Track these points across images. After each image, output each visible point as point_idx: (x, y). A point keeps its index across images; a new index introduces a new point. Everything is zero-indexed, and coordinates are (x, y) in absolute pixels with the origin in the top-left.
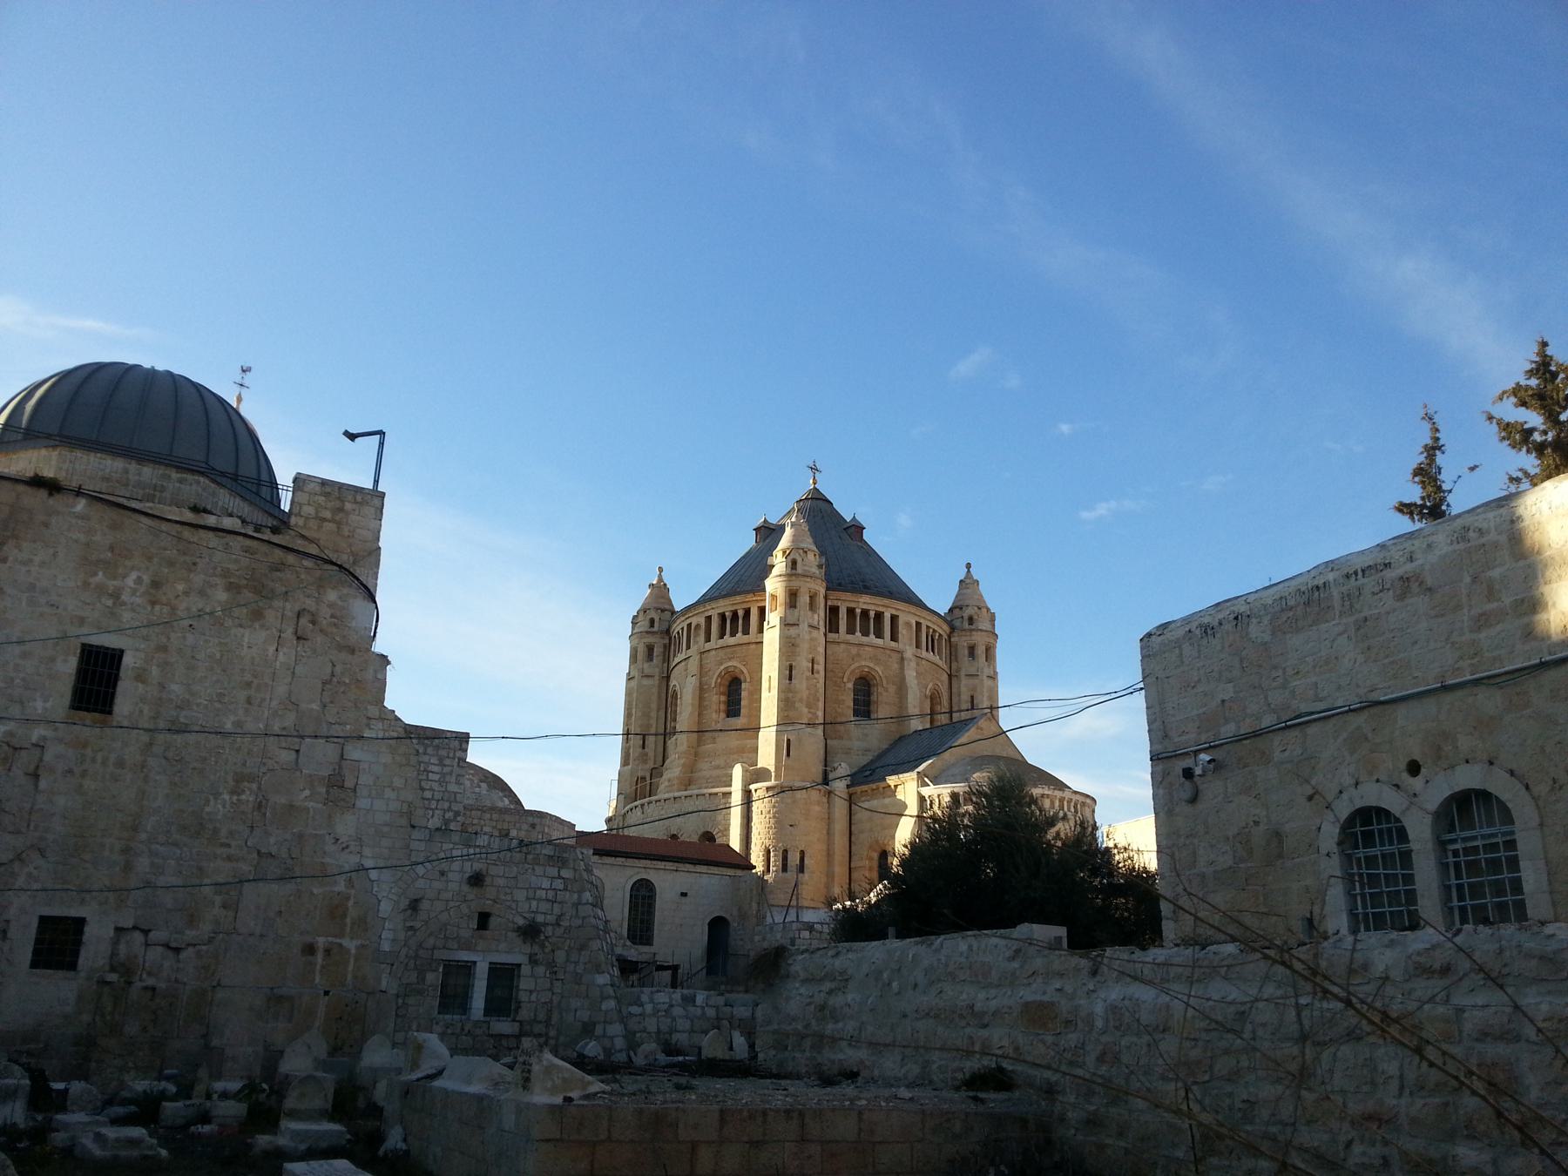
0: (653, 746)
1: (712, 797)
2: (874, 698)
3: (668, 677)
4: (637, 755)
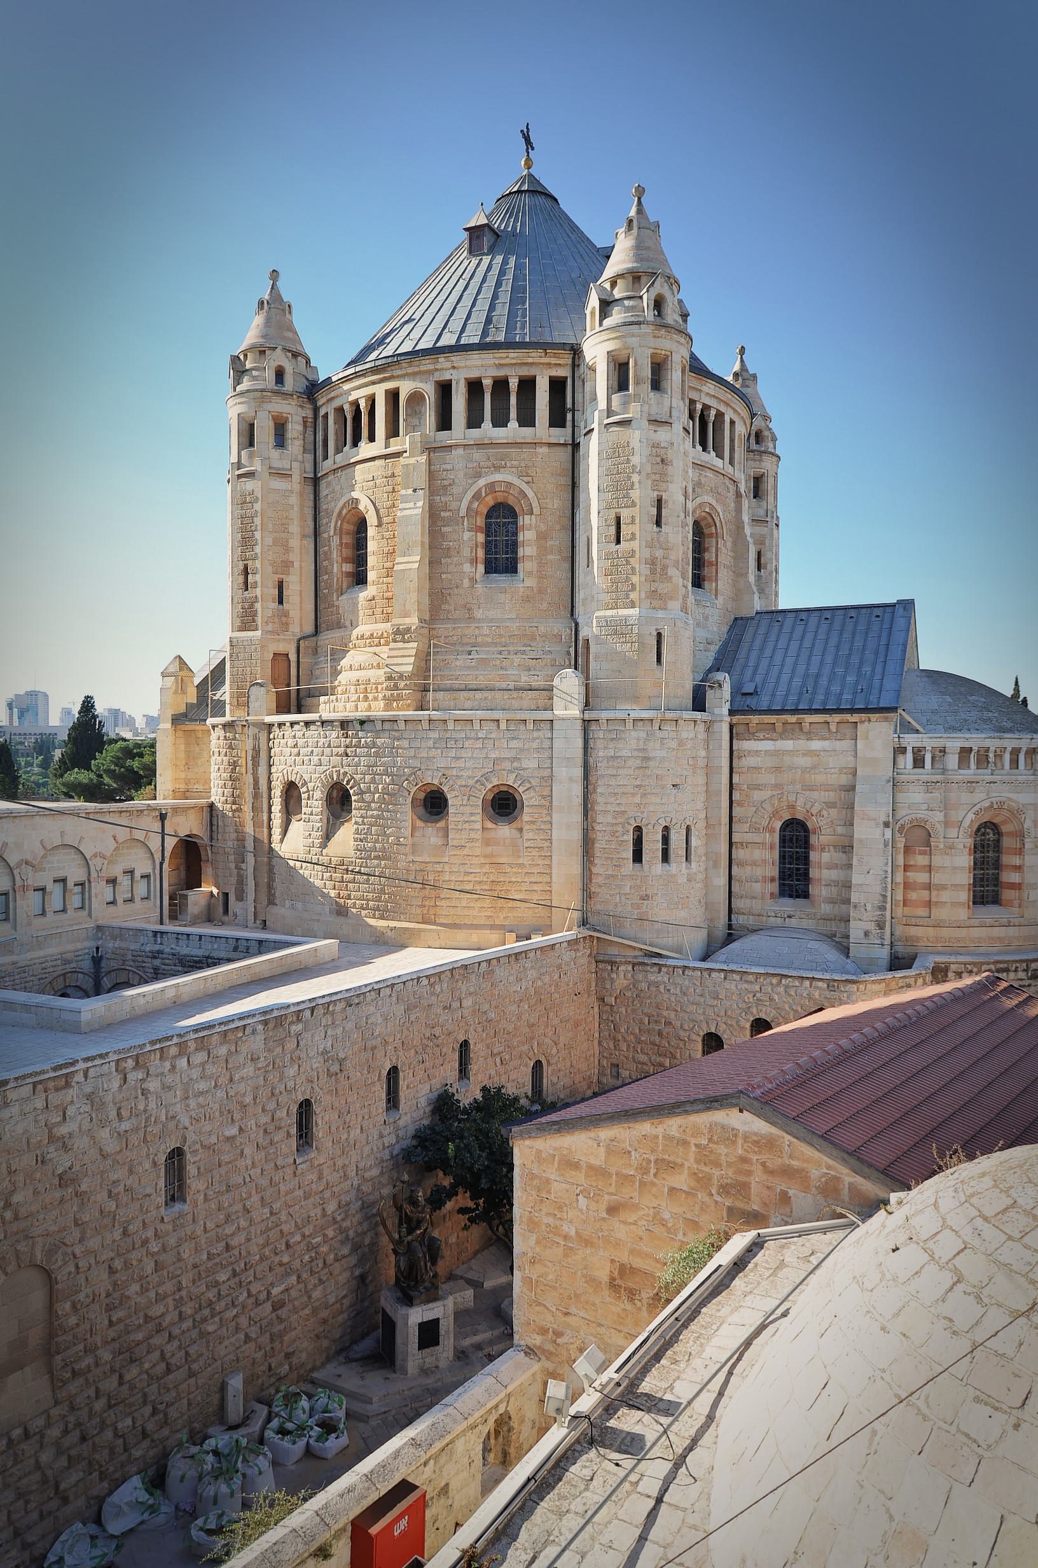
2: (709, 556)
3: (315, 481)
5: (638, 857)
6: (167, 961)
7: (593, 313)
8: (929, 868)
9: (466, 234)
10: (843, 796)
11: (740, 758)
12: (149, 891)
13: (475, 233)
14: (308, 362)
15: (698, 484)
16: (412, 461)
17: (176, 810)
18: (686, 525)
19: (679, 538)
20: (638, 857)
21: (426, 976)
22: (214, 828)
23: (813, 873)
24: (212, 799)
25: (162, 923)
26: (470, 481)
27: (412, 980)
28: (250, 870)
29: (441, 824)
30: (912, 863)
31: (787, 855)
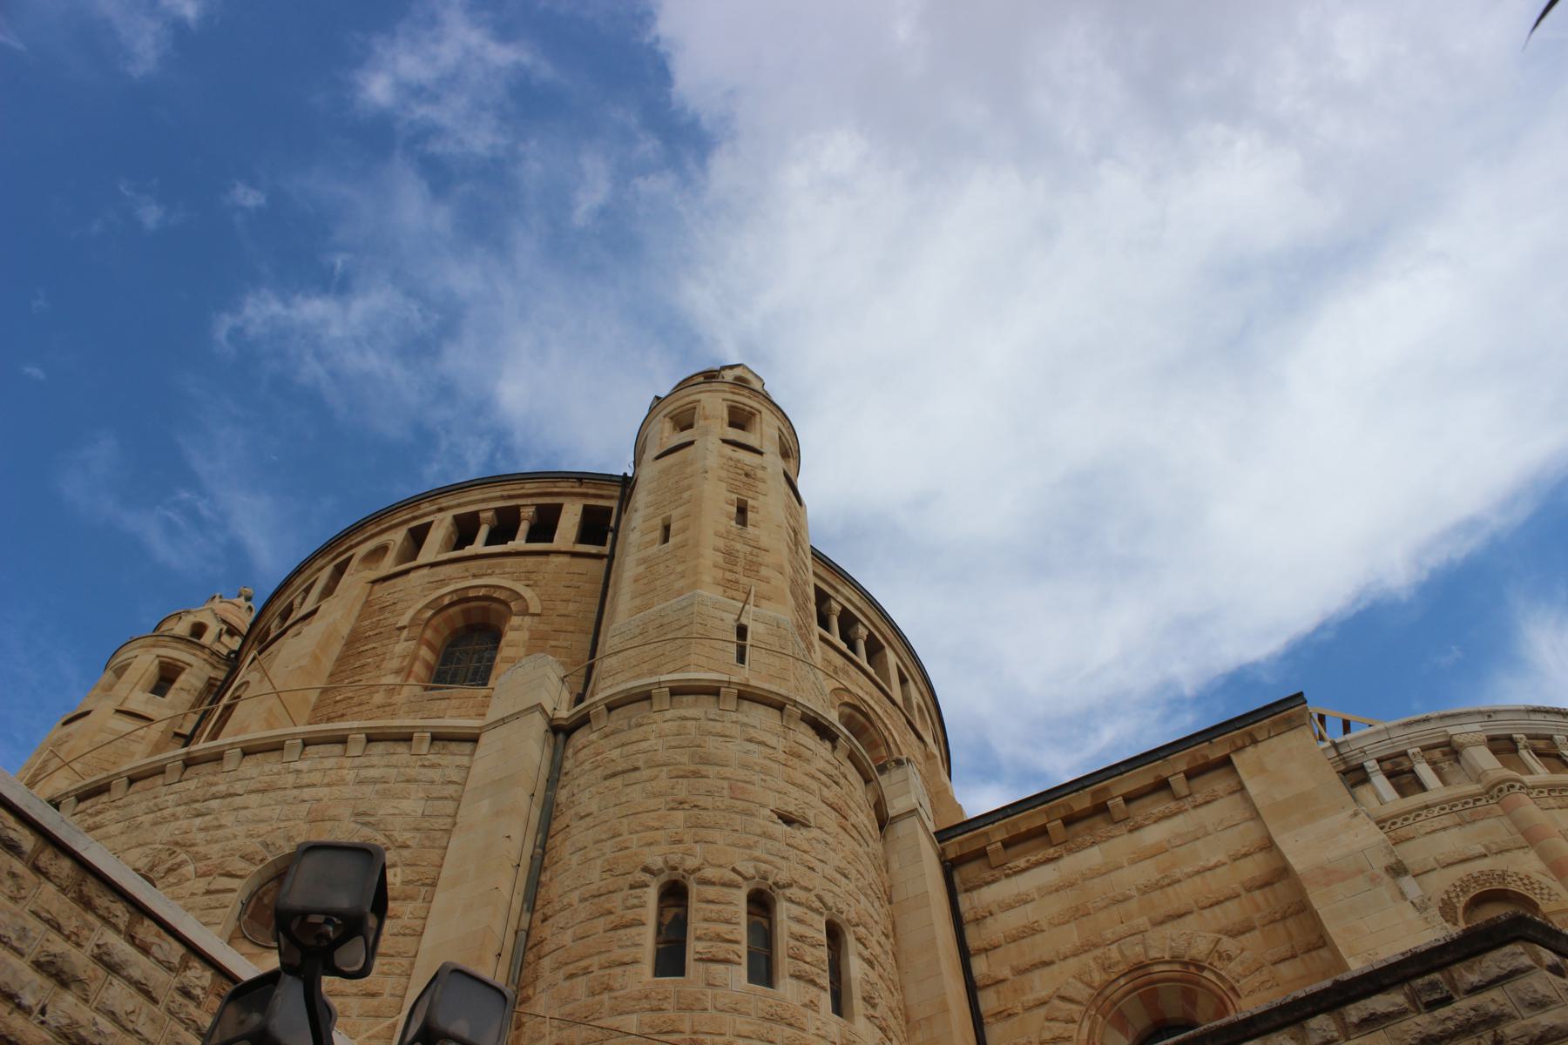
1: (379, 748)
5: (671, 959)
11: (978, 920)
20: (671, 959)
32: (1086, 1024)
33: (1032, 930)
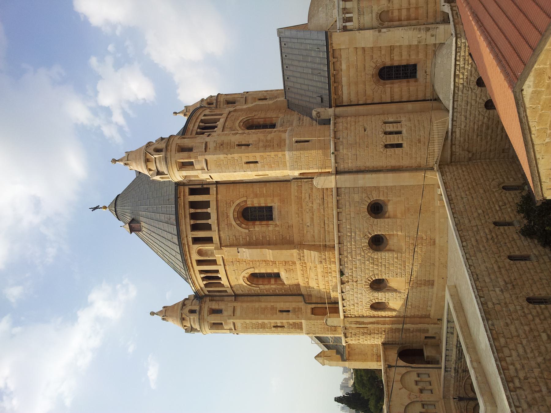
0: (287, 304)
1: (340, 206)
2: (261, 121)
3: (236, 296)
4: (294, 316)
5: (399, 146)
6: (460, 366)
7: (162, 178)
8: (400, 10)
9: (133, 233)
10: (367, 53)
11: (351, 101)
12: (425, 374)
13: (132, 230)
14: (186, 299)
15: (231, 129)
16: (226, 253)
17: (385, 360)
18: (249, 134)
19: (253, 136)
20: (399, 146)
21: (462, 243)
22: (394, 343)
23: (404, 63)
24: (380, 343)
25: (441, 368)
26: (233, 229)
27: (464, 250)
28: (413, 326)
29: (387, 237)
30: (397, 18)
31: (396, 76)
32: (379, 86)
33: (357, 93)
